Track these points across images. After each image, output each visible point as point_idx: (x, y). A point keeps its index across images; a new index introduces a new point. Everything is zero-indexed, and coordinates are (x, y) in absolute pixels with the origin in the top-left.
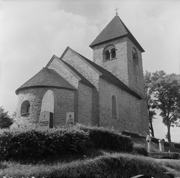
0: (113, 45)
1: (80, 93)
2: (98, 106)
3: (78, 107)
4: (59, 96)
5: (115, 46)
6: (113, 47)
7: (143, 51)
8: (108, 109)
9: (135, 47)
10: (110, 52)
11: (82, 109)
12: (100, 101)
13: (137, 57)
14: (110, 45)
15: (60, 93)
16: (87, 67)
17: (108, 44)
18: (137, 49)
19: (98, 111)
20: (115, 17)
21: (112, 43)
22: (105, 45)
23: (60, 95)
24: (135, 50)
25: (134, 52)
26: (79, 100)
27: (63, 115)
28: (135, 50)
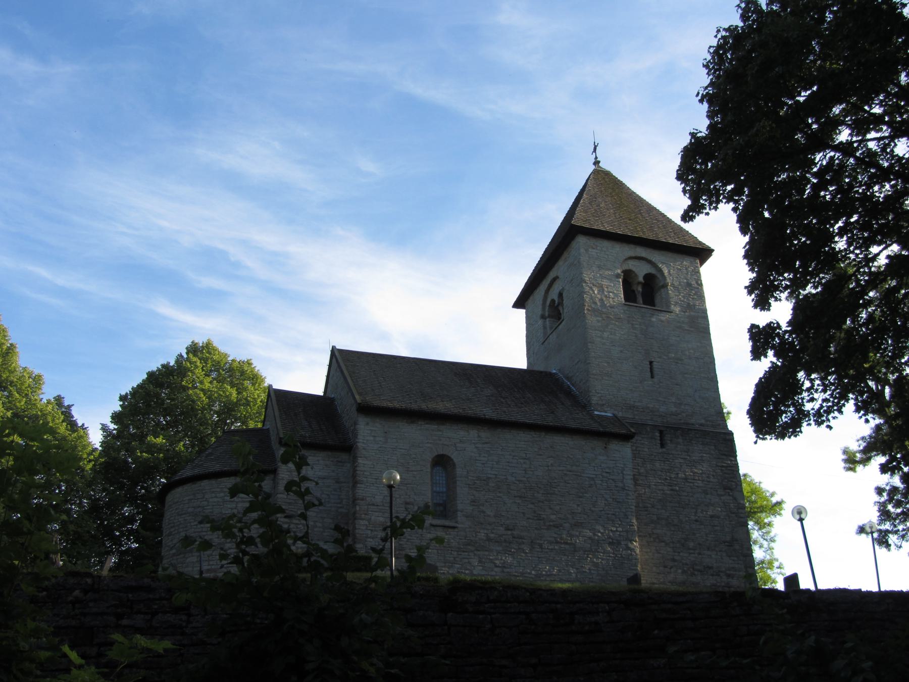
2: (355, 501)
4: (216, 500)
8: (407, 503)
12: (358, 485)
13: (665, 286)
15: (218, 490)
18: (656, 256)
23: (218, 495)
25: (641, 270)
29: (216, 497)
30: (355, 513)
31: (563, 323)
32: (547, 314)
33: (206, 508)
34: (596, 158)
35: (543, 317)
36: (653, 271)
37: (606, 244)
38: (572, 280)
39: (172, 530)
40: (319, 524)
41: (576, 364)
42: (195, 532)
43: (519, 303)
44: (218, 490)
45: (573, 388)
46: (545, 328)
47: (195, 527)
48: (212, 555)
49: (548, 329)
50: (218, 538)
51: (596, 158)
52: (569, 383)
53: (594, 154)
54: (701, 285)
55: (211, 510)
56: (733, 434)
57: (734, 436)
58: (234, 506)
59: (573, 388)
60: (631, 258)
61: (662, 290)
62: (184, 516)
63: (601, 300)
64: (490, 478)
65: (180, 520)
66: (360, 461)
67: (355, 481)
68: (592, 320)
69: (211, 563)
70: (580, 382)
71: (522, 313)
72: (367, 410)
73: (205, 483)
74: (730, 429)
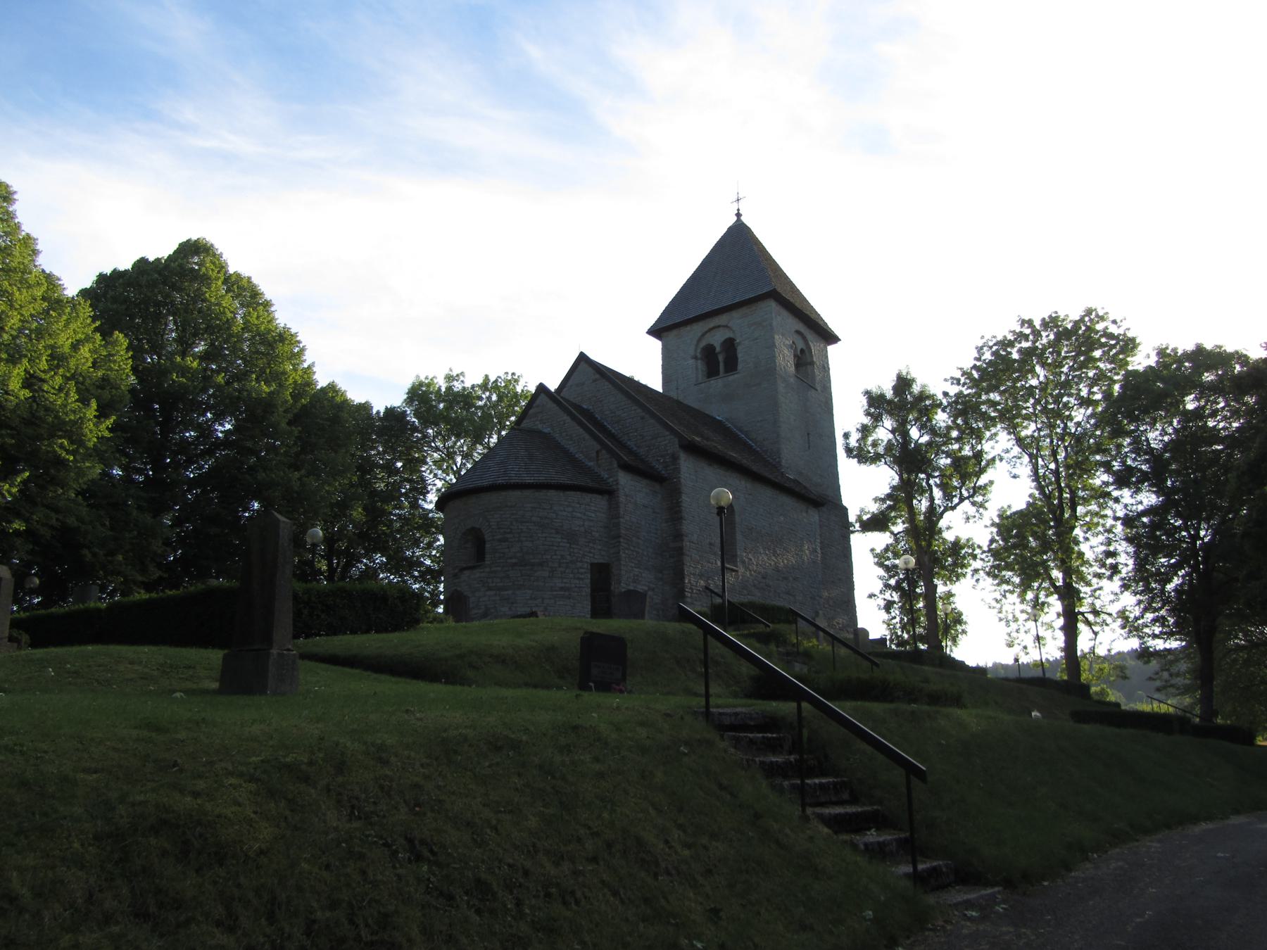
0: (726, 326)
1: (622, 499)
2: (678, 536)
3: (620, 542)
4: (565, 514)
5: (734, 332)
6: (728, 334)
7: (831, 338)
8: (711, 544)
9: (801, 327)
10: (718, 349)
11: (632, 548)
12: (684, 521)
13: (812, 363)
14: (719, 326)
15: (566, 503)
16: (642, 418)
17: (712, 325)
18: (810, 336)
19: (680, 552)
20: (731, 230)
21: (722, 319)
22: (698, 328)
24: (804, 338)
25: (800, 345)
26: (621, 520)
27: (579, 564)
28: (804, 338)
29: (565, 511)
30: (681, 548)
31: (736, 376)
32: (699, 355)
33: (555, 520)
34: (738, 210)
35: (695, 358)
36: (804, 348)
37: (785, 313)
38: (757, 339)
39: (508, 536)
40: (645, 553)
41: (758, 422)
42: (543, 545)
43: (656, 331)
44: (566, 503)
45: (750, 442)
46: (697, 369)
47: (544, 539)
48: (565, 573)
49: (700, 370)
50: (570, 555)
51: (738, 210)
52: (743, 436)
53: (736, 204)
54: (829, 369)
55: (561, 524)
56: (847, 509)
57: (849, 511)
58: (582, 523)
59: (750, 442)
60: (798, 332)
61: (808, 366)
62: (527, 524)
63: (784, 367)
64: (753, 528)
65: (520, 527)
66: (684, 497)
67: (675, 513)
68: (781, 387)
69: (565, 581)
70: (764, 440)
71: (656, 345)
72: (692, 449)
73: (552, 493)
74: (844, 504)
